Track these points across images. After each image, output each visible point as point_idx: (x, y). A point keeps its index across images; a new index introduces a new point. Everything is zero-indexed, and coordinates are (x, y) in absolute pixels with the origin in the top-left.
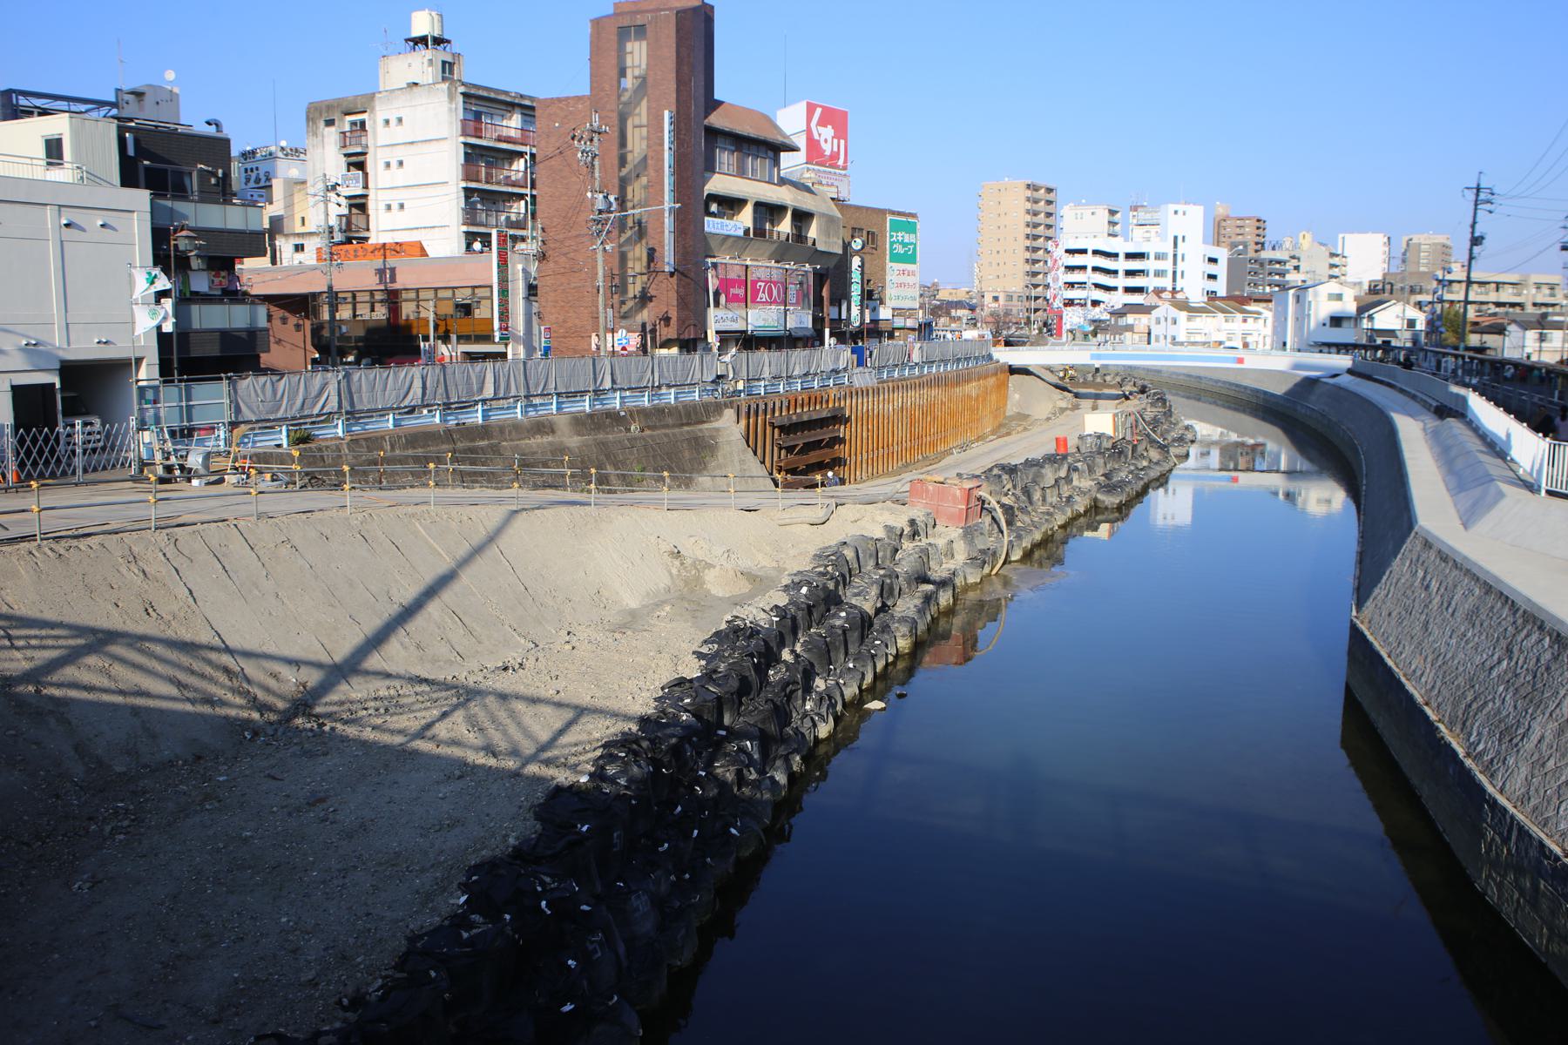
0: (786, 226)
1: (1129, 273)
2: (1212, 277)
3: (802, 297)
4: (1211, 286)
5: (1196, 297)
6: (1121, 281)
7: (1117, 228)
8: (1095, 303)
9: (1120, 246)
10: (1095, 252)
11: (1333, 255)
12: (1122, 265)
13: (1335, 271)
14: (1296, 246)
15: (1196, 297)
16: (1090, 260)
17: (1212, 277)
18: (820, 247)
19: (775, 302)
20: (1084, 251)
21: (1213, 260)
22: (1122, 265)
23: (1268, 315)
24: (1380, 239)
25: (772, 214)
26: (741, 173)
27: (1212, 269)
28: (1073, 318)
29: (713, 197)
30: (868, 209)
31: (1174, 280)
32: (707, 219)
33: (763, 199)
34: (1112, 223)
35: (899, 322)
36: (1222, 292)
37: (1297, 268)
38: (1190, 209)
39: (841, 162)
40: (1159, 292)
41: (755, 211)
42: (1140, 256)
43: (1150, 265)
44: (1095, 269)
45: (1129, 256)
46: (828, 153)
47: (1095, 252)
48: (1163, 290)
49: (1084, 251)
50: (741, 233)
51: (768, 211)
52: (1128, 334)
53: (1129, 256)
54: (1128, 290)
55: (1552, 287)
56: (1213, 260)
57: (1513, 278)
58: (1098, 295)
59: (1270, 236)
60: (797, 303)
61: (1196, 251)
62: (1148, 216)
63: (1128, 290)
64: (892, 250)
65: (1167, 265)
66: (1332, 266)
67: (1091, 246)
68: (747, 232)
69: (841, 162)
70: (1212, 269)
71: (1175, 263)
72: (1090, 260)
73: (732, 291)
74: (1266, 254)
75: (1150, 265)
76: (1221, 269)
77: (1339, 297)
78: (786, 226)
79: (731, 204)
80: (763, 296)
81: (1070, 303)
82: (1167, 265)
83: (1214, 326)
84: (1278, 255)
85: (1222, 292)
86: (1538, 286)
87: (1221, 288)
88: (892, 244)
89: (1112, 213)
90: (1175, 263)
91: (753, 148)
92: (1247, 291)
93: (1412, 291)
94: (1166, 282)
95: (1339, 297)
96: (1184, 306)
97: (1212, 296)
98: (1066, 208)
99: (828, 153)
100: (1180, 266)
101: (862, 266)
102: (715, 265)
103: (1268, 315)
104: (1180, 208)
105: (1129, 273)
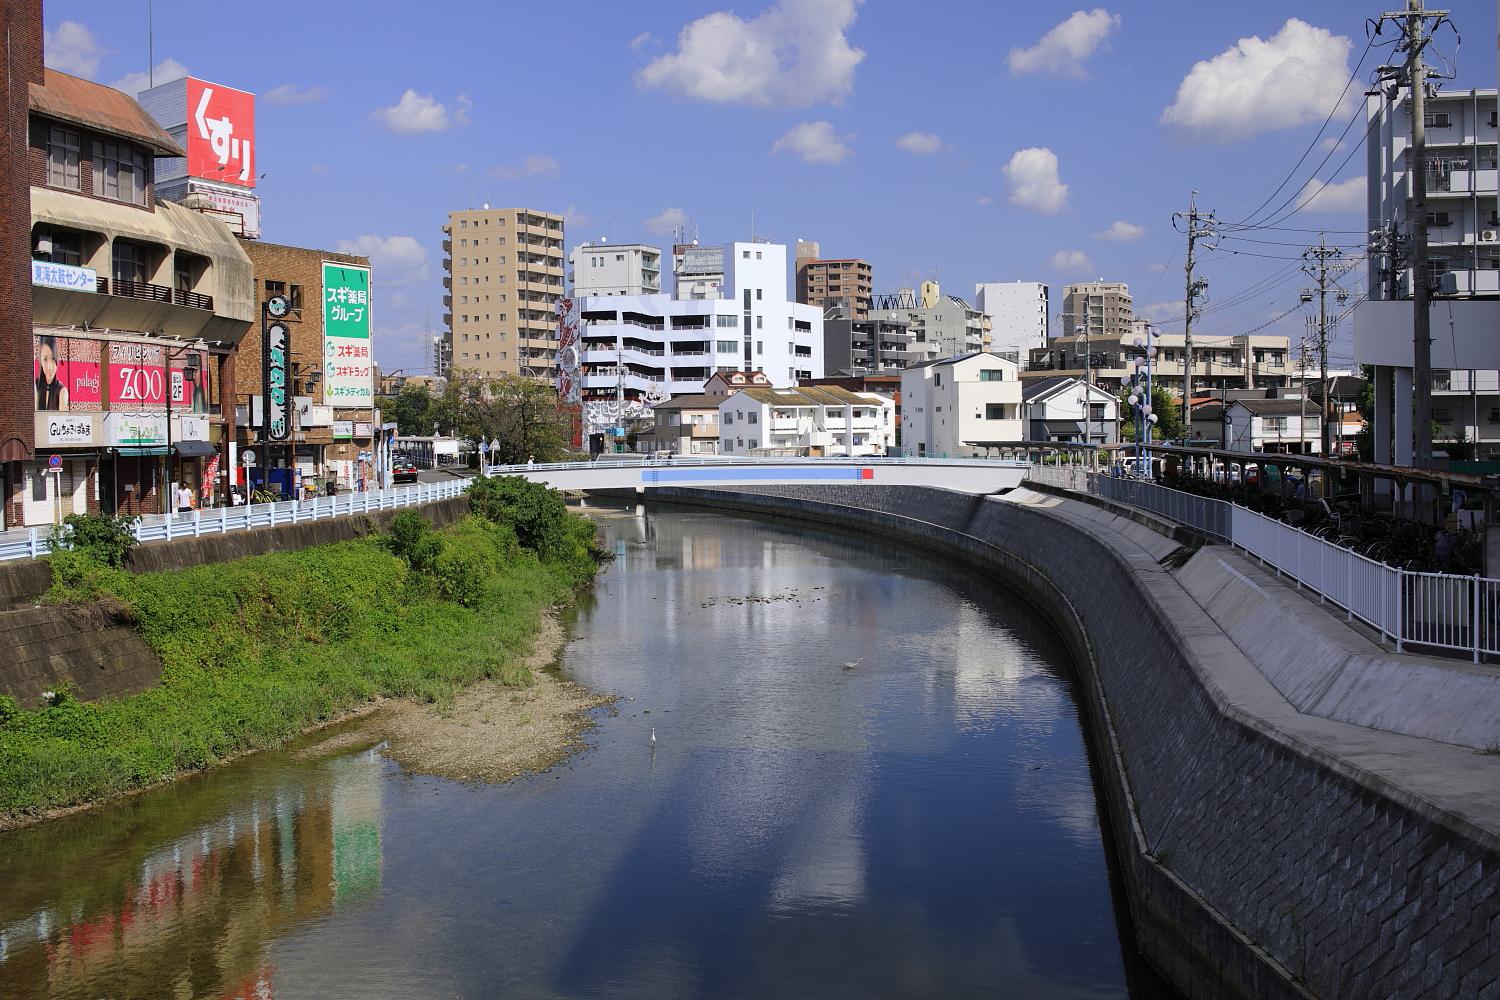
0: (165, 275)
1: (680, 348)
2: (803, 351)
3: (195, 390)
4: (802, 363)
5: (781, 380)
6: (668, 361)
7: (657, 279)
8: (632, 394)
9: (662, 305)
10: (629, 317)
11: (971, 315)
12: (669, 335)
13: (975, 339)
14: (919, 301)
15: (781, 380)
16: (620, 329)
17: (803, 351)
18: (220, 310)
19: (150, 399)
20: (612, 315)
21: (803, 326)
22: (669, 335)
23: (889, 403)
24: (1033, 290)
25: (142, 258)
26: (86, 190)
27: (802, 339)
28: (599, 417)
29: (45, 230)
30: (290, 250)
31: (748, 355)
32: (35, 264)
33: (128, 233)
34: (649, 274)
35: (342, 430)
36: (818, 373)
37: (921, 337)
38: (767, 248)
39: (244, 176)
40: (727, 374)
41: (115, 253)
42: (697, 321)
43: (714, 333)
44: (629, 342)
45: (680, 322)
46: (224, 161)
47: (629, 317)
48: (734, 371)
49: (612, 315)
50: (92, 287)
51: (138, 254)
52: (685, 441)
53: (680, 322)
54: (679, 373)
55: (1278, 353)
56: (803, 326)
57: (1225, 342)
58: (633, 381)
59: (879, 288)
60: (187, 401)
61: (778, 309)
62: (701, 261)
63: (679, 373)
64: (330, 316)
65: (736, 334)
66: (971, 331)
67: (621, 306)
68: (103, 285)
69: (244, 176)
70: (802, 339)
71: (748, 330)
72: (620, 329)
73: (80, 382)
74: (876, 315)
75: (714, 333)
76: (815, 339)
77: (994, 375)
78: (165, 275)
79: (75, 243)
80: (130, 391)
81: (592, 394)
82: (736, 334)
83: (823, 430)
84: (893, 316)
85: (818, 373)
86: (1259, 353)
87: (816, 366)
88: (329, 308)
89: (648, 257)
90: (748, 330)
91: (111, 150)
92: (854, 372)
93: (1101, 362)
94: (736, 360)
95: (994, 375)
96: (767, 394)
97: (804, 378)
98: (578, 250)
99: (224, 161)
100: (756, 335)
101: (286, 342)
102: (50, 341)
103: (889, 403)
104: (753, 248)
105: (680, 348)
